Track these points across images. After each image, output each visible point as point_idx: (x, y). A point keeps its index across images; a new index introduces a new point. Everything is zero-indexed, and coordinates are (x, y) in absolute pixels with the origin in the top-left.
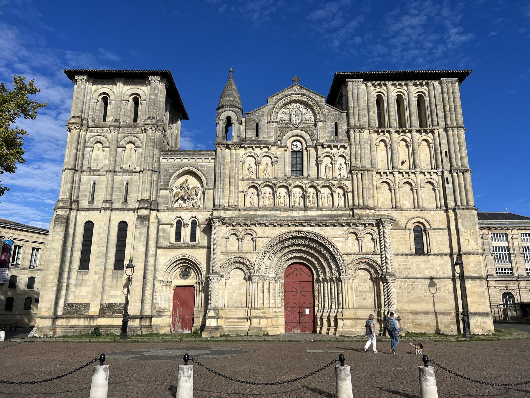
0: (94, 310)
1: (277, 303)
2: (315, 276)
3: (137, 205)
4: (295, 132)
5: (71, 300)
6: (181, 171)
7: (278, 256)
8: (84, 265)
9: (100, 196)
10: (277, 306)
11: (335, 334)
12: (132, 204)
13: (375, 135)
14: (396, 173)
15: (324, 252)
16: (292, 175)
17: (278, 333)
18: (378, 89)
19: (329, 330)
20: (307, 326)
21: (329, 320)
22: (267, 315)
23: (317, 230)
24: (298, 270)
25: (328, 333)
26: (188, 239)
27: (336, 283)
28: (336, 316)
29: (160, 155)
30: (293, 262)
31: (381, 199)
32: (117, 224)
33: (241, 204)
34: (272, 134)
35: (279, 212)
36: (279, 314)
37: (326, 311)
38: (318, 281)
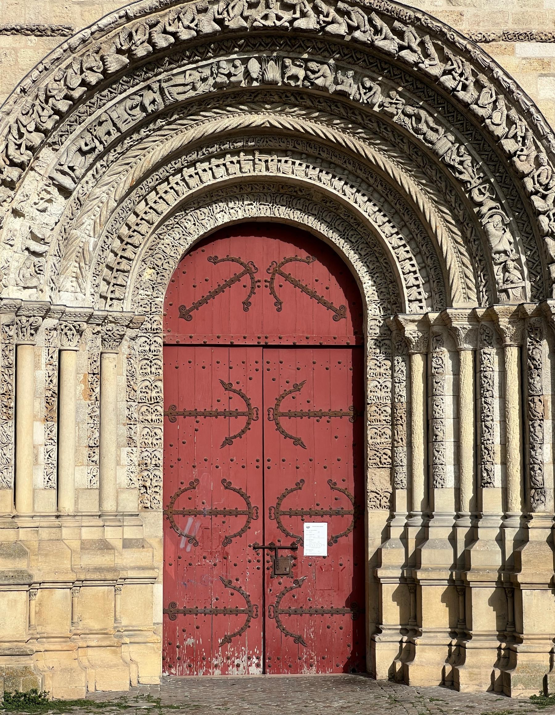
1: (109, 490)
2: (374, 312)
7: (119, 177)
10: (109, 506)
11: (502, 686)
15: (444, 143)
17: (112, 681)
19: (457, 657)
20: (309, 633)
21: (459, 593)
22: (40, 570)
24: (262, 275)
25: (451, 682)
27: (513, 354)
28: (512, 565)
30: (223, 219)
36: (129, 558)
37: (439, 532)
38: (395, 343)
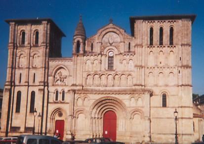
0: (22, 129)
3: (39, 84)
4: (110, 47)
5: (13, 125)
6: (58, 67)
8: (18, 110)
9: (24, 79)
12: (37, 83)
13: (146, 49)
14: (156, 68)
16: (108, 68)
18: (151, 24)
23: (117, 96)
26: (61, 100)
29: (48, 59)
31: (150, 83)
32: (30, 93)
33: (84, 84)
34: (99, 49)
35: (100, 87)
